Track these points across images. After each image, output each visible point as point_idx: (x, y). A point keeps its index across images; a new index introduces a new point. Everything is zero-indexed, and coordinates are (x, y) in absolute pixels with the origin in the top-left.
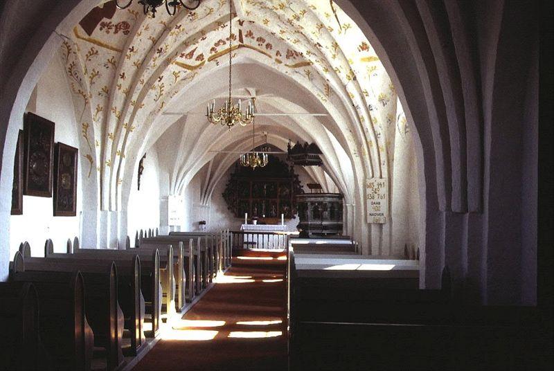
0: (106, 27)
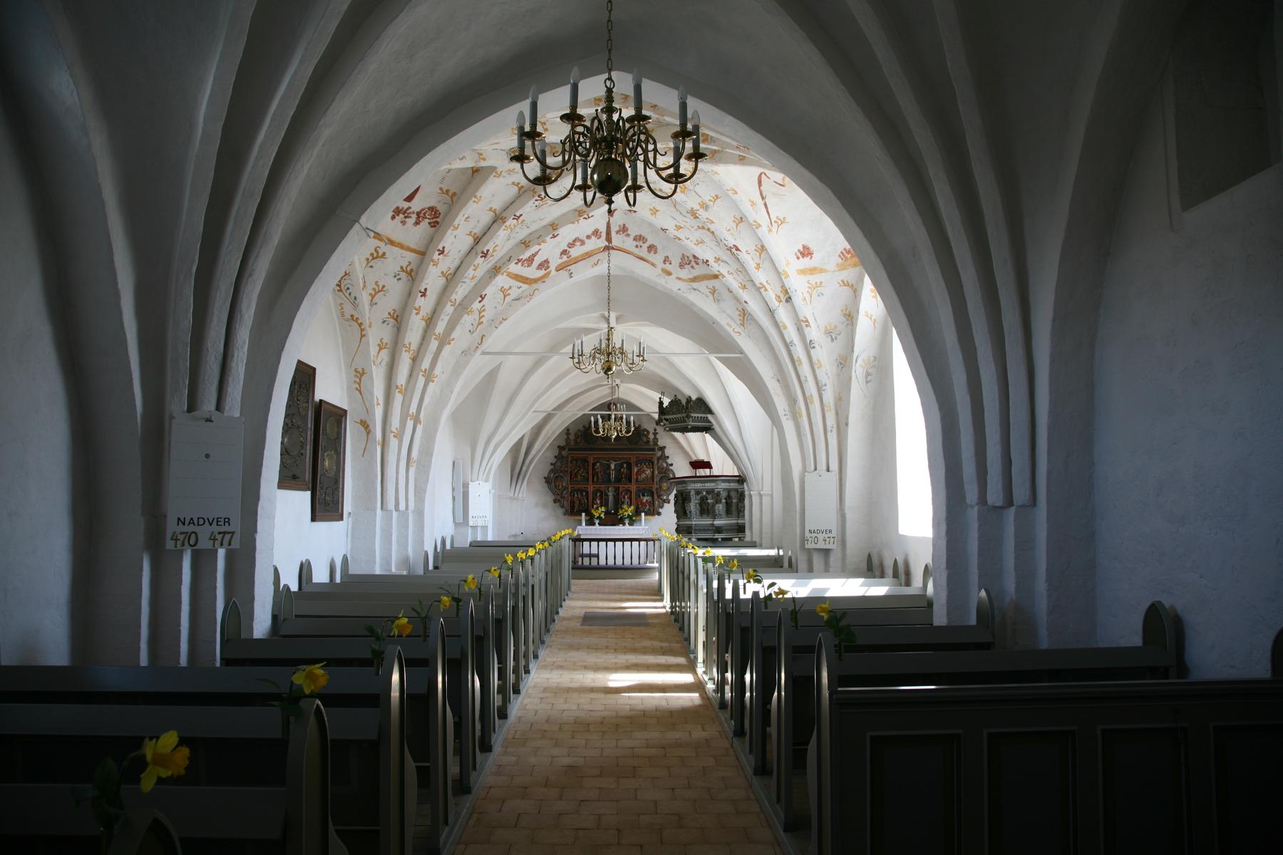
0: (401, 216)
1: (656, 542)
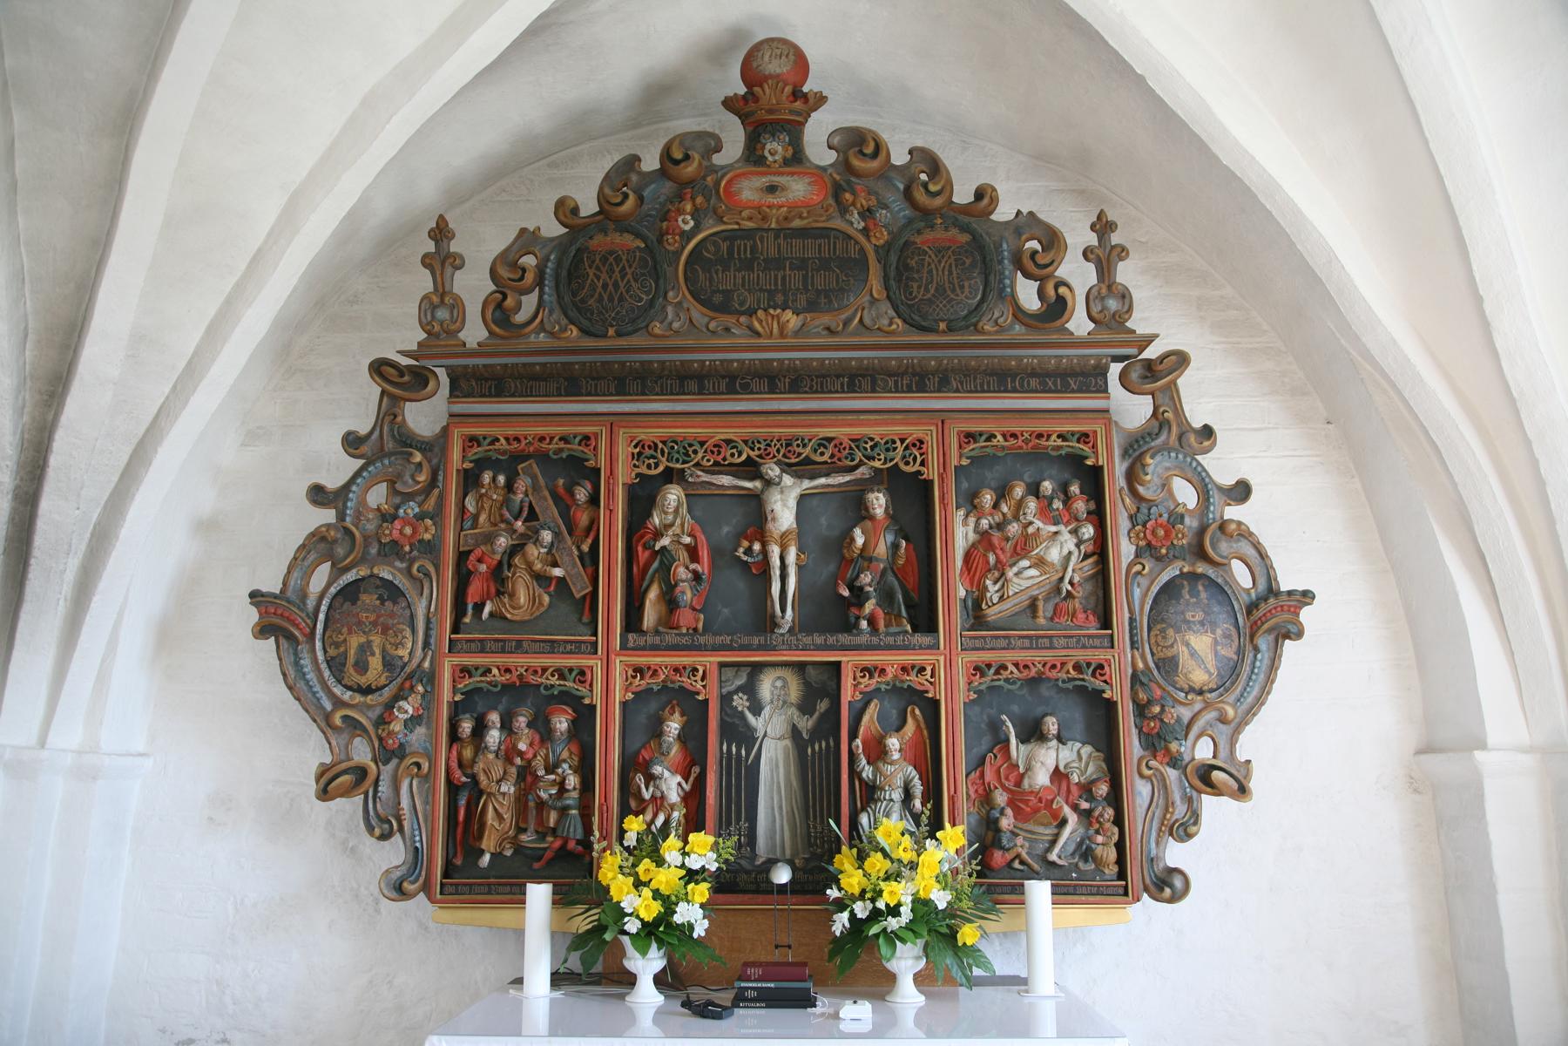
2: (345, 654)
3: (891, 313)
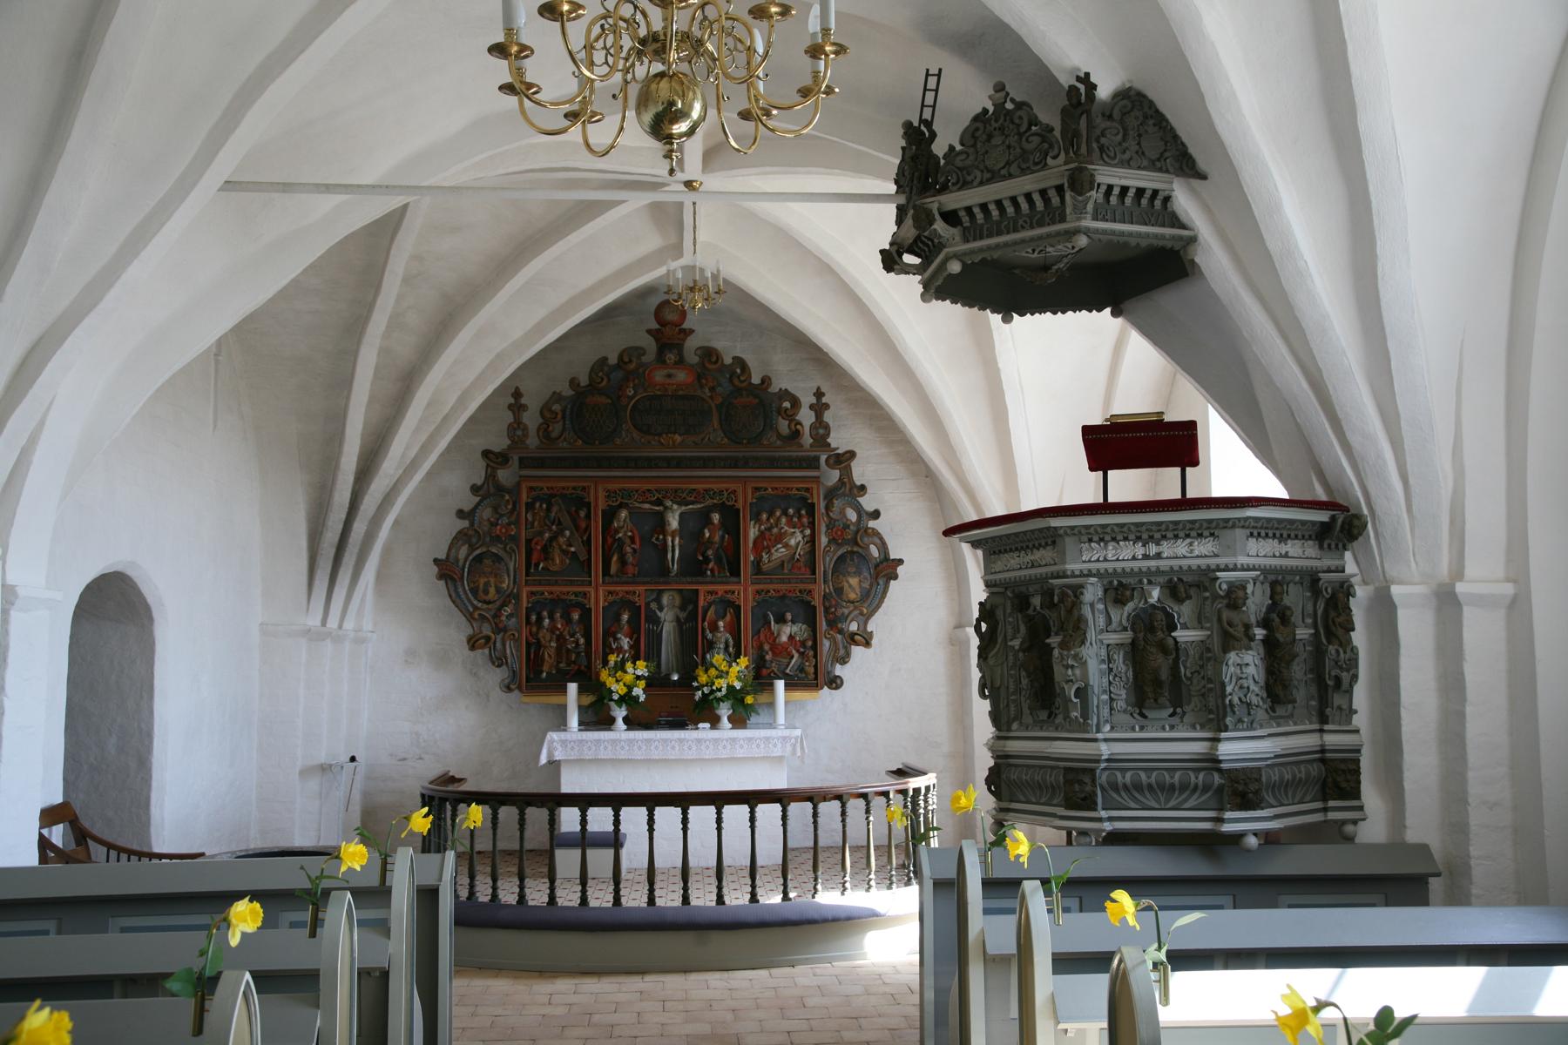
1: (855, 806)
2: (479, 586)
3: (722, 435)
